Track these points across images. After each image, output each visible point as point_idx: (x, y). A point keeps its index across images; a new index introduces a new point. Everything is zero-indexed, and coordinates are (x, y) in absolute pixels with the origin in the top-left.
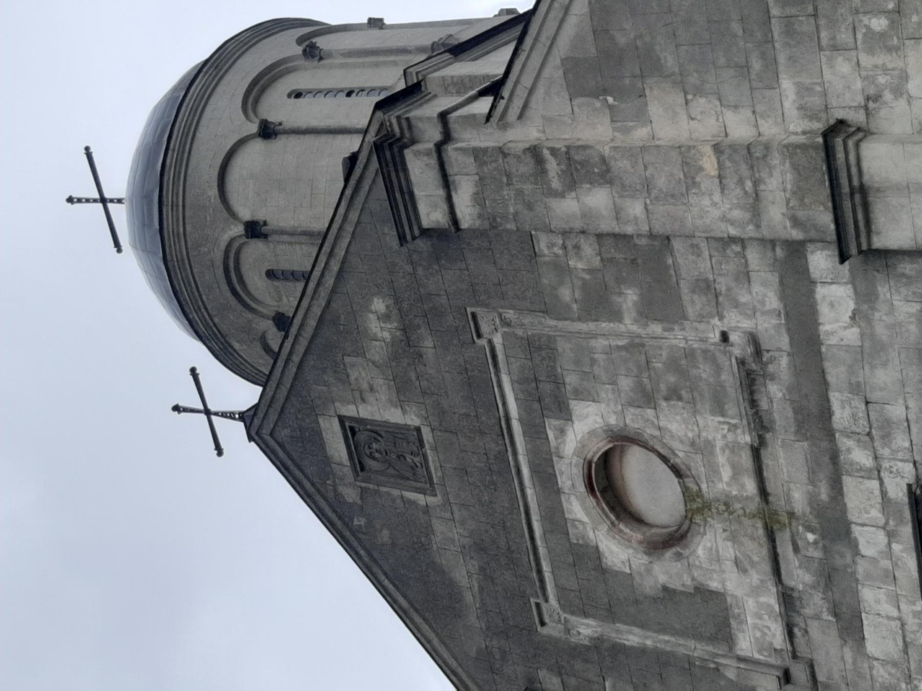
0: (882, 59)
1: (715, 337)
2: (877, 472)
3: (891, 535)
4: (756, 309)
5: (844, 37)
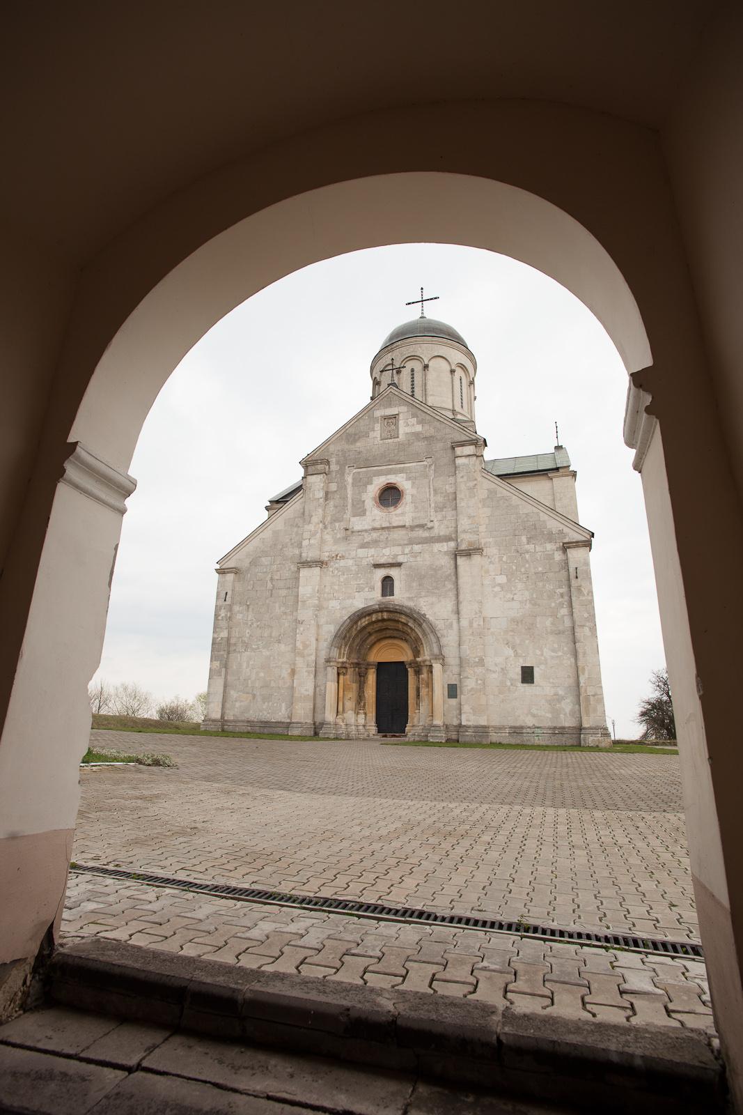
0: (497, 560)
2: (403, 554)
4: (440, 529)
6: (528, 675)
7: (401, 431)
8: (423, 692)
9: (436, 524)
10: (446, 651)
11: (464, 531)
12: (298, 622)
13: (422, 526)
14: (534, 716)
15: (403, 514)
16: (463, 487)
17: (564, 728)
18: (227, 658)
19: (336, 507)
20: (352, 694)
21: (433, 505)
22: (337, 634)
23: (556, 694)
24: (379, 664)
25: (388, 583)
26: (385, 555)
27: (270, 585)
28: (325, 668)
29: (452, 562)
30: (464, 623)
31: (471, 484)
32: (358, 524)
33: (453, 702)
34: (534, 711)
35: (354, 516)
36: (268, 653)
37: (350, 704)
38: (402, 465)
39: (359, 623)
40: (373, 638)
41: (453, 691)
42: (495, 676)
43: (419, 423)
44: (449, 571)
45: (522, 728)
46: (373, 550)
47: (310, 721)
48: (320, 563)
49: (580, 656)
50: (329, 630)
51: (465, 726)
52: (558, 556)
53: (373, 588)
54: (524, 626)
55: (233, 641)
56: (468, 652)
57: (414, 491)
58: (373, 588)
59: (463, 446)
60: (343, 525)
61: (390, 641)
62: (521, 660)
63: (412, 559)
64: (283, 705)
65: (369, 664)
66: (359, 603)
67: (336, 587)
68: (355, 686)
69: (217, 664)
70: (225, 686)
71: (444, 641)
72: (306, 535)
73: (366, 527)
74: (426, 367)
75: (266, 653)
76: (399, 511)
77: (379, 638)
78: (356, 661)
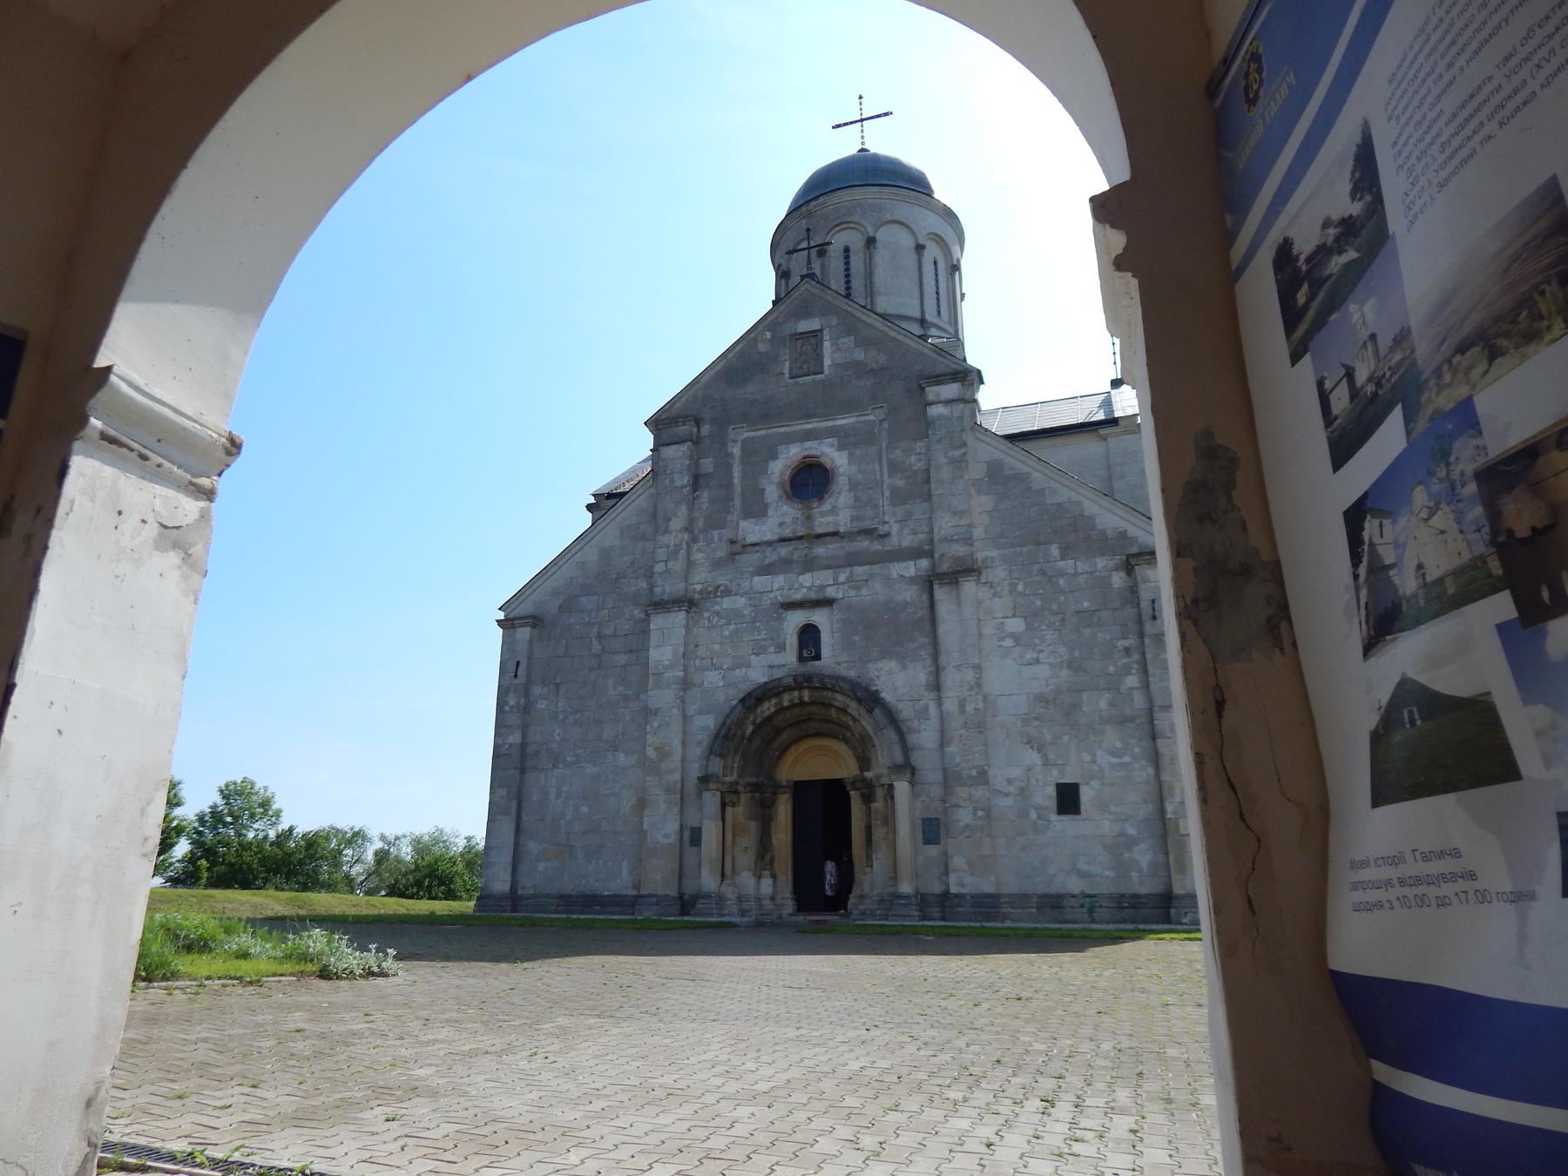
1: (887, 518)
2: (836, 583)
3: (810, 588)
4: (901, 537)
5: (1015, 575)
6: (1068, 799)
7: (827, 362)
8: (879, 833)
9: (895, 529)
10: (917, 759)
11: (948, 540)
12: (648, 713)
13: (869, 533)
14: (1083, 875)
15: (834, 511)
16: (941, 459)
17: (1137, 896)
18: (522, 781)
19: (712, 501)
20: (749, 841)
21: (887, 494)
22: (719, 731)
23: (1122, 834)
25: (809, 636)
26: (807, 583)
27: (596, 646)
28: (700, 794)
29: (925, 597)
30: (950, 705)
31: (958, 453)
32: (753, 531)
33: (933, 851)
34: (1082, 866)
35: (745, 518)
36: (596, 770)
37: (745, 858)
38: (831, 423)
39: (759, 710)
41: (932, 831)
42: (1007, 801)
43: (857, 345)
44: (920, 613)
45: (1060, 896)
46: (781, 578)
47: (673, 893)
48: (689, 603)
49: (1165, 761)
50: (706, 723)
51: (956, 895)
52: (1118, 580)
53: (781, 648)
54: (1058, 707)
55: (531, 750)
56: (958, 759)
57: (854, 468)
58: (781, 648)
59: (939, 383)
60: (727, 533)
61: (816, 742)
62: (1055, 772)
63: (852, 593)
64: (624, 864)
66: (757, 674)
67: (716, 647)
68: (753, 826)
69: (503, 792)
70: (518, 831)
71: (913, 739)
72: (661, 553)
73: (769, 537)
74: (871, 242)
75: (591, 769)
76: (826, 506)
78: (754, 780)
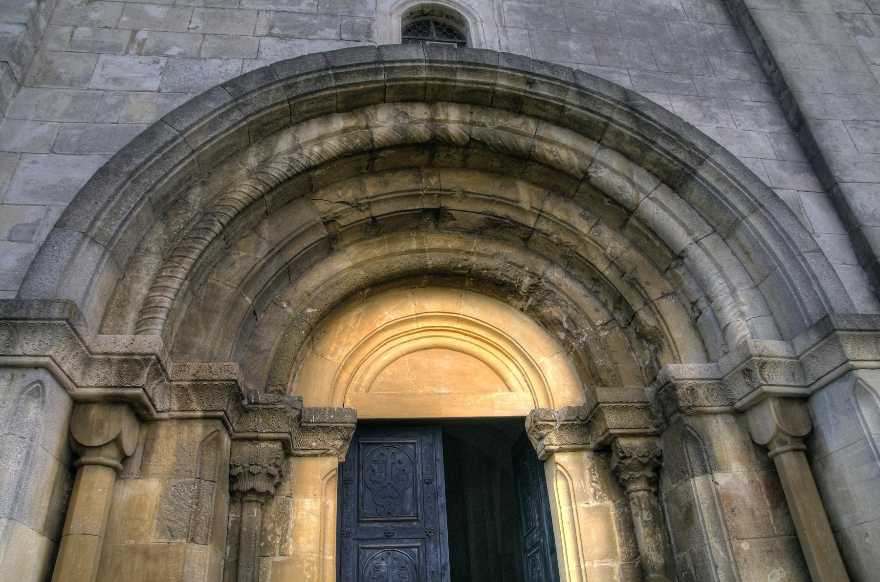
24: (370, 431)
39: (284, 143)
40: (346, 265)
65: (303, 422)
77: (380, 268)
